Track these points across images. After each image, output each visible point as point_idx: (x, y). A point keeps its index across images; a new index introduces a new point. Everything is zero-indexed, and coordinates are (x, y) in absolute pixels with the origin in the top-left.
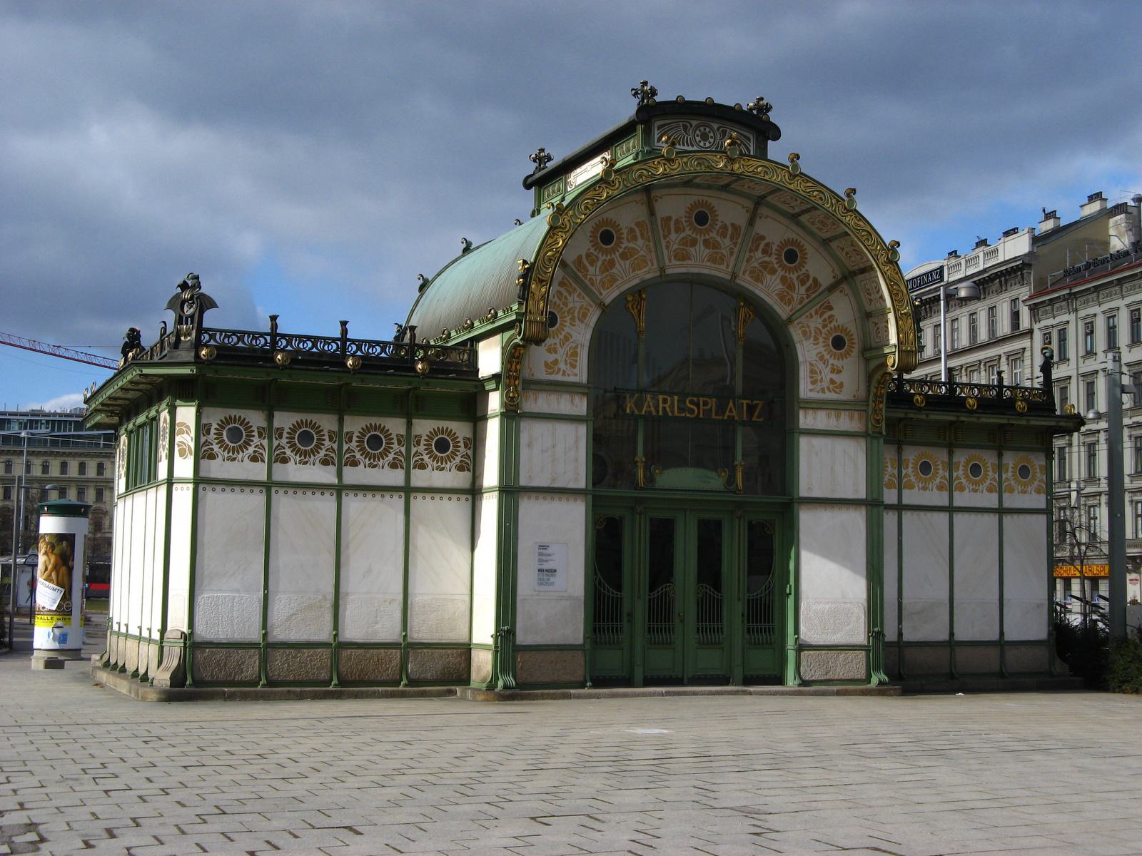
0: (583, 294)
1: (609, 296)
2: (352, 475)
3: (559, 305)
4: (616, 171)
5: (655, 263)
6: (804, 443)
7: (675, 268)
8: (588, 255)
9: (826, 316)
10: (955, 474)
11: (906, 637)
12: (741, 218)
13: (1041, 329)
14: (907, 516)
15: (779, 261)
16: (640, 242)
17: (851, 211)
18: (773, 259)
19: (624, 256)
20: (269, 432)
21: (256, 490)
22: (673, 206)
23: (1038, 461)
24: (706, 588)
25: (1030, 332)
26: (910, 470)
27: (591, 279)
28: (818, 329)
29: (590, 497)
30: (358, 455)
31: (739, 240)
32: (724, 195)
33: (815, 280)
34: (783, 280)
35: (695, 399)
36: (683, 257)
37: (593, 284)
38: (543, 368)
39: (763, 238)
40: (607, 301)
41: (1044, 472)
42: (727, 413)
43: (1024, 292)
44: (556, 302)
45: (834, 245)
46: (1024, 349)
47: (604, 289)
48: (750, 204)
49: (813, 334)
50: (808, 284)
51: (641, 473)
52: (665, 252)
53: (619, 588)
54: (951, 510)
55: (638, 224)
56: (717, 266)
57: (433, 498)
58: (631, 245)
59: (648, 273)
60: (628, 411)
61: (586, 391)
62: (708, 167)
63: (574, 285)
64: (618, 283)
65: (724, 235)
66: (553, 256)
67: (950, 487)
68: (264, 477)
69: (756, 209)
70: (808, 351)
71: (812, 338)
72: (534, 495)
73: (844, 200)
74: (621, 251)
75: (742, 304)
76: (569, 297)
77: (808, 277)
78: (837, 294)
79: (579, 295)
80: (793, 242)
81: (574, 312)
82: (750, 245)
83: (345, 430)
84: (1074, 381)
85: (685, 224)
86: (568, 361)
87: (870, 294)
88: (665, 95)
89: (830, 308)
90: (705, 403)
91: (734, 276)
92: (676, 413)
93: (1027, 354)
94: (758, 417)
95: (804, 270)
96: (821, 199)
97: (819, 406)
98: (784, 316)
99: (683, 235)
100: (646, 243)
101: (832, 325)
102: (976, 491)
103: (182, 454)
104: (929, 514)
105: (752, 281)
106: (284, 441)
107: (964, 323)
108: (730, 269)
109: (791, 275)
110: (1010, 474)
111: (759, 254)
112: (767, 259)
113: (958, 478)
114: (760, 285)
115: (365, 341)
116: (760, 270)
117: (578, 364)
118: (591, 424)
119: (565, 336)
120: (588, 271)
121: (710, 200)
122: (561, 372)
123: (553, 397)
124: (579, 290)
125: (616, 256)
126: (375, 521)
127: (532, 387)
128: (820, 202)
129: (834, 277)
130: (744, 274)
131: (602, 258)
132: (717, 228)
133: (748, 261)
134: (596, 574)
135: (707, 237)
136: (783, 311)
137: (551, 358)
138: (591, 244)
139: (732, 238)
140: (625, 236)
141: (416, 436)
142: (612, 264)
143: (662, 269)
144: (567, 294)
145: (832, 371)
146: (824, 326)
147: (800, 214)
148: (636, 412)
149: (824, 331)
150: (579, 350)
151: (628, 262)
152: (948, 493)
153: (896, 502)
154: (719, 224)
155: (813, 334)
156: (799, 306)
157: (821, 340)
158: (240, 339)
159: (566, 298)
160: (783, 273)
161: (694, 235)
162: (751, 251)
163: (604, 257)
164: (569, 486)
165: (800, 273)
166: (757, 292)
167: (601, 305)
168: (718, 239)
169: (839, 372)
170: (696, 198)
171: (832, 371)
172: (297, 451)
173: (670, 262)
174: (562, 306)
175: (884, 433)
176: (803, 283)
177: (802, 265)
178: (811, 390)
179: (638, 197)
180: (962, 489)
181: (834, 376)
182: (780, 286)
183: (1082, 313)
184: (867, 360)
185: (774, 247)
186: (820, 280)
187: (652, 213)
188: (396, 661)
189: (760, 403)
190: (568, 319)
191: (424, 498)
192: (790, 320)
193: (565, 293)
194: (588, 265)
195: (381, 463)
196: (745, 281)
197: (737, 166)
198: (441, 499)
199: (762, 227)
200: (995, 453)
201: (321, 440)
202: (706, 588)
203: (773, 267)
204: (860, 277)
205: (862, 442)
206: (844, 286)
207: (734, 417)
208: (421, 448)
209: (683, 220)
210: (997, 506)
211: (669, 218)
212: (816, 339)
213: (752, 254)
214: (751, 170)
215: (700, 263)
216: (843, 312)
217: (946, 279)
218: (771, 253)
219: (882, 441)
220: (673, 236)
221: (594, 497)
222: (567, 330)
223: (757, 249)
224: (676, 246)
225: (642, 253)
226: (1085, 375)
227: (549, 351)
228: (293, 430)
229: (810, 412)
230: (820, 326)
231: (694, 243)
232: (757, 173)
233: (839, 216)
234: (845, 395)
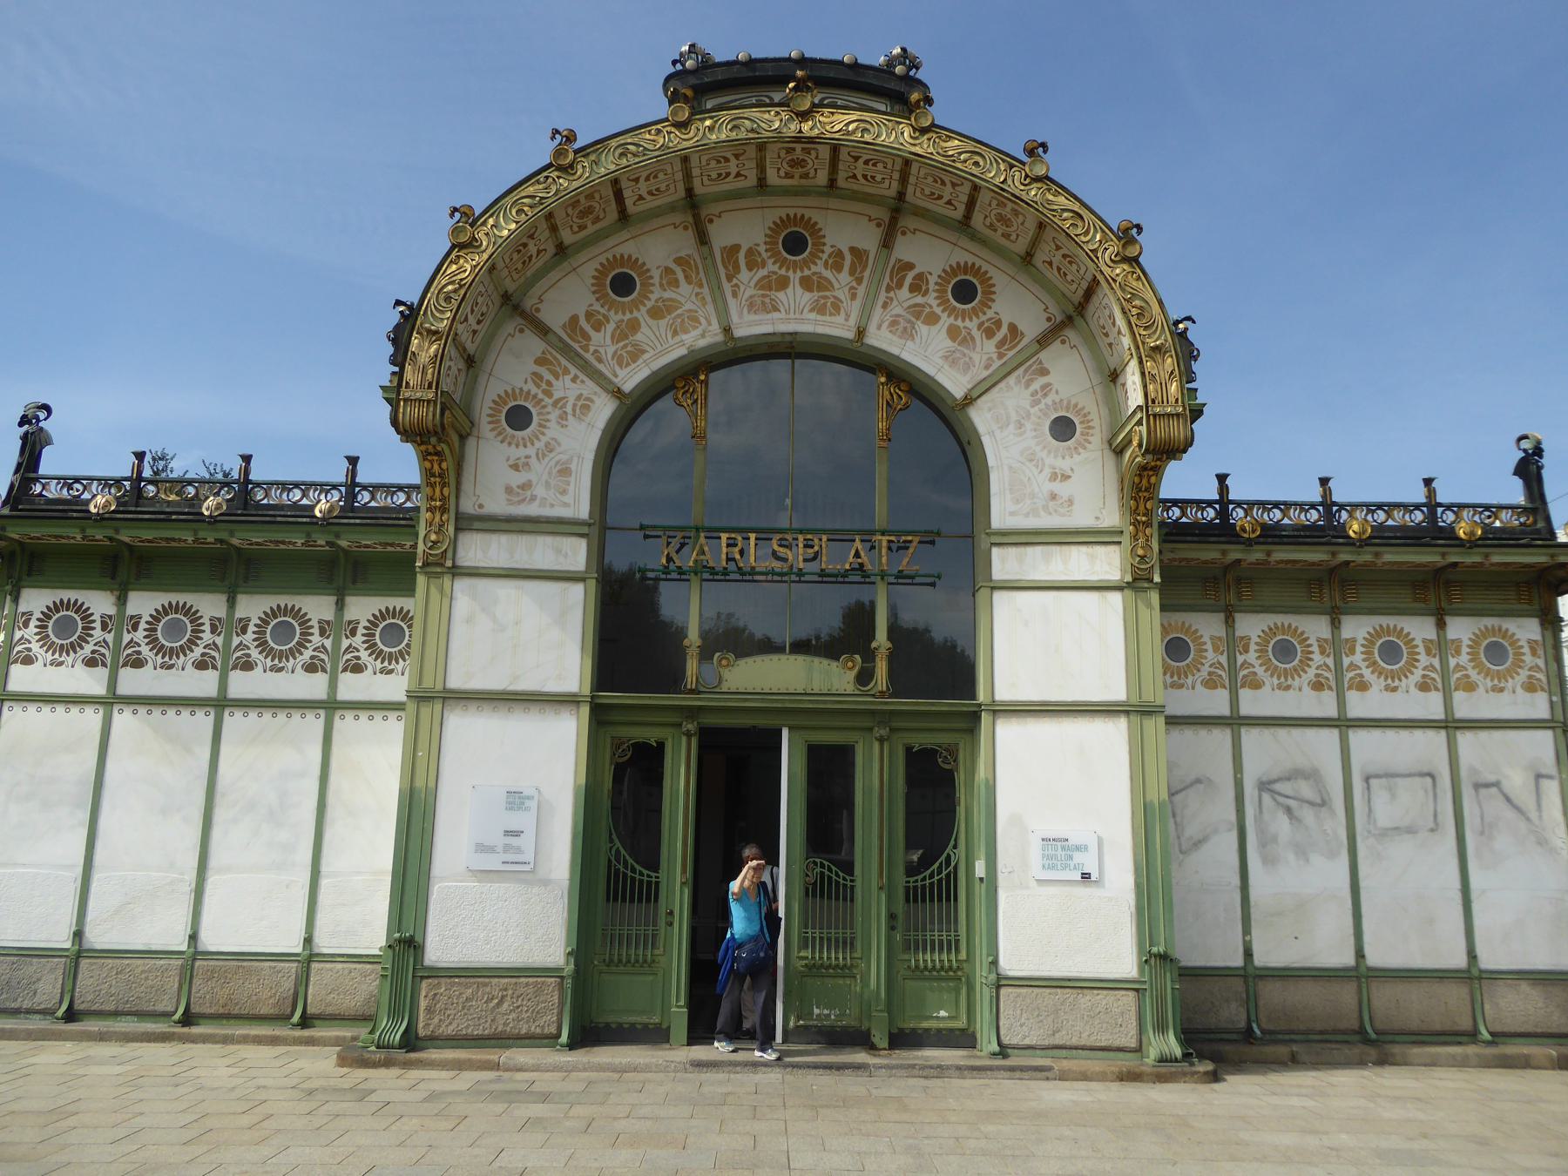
0: (582, 376)
1: (631, 378)
2: (242, 685)
3: (535, 396)
4: (576, 152)
5: (714, 321)
7: (751, 326)
8: (589, 315)
9: (1036, 385)
10: (1346, 661)
11: (1260, 960)
12: (869, 239)
14: (1249, 736)
15: (944, 302)
16: (685, 288)
17: (1037, 179)
18: (932, 299)
19: (656, 313)
20: (119, 622)
21: (89, 710)
22: (742, 229)
23: (1527, 630)
24: (822, 866)
26: (1252, 656)
27: (596, 351)
29: (585, 710)
30: (255, 654)
31: (867, 273)
32: (834, 203)
33: (1013, 328)
34: (953, 333)
35: (789, 537)
37: (600, 360)
38: (504, 496)
39: (910, 266)
40: (628, 387)
41: (1540, 652)
44: (529, 392)
45: (1039, 259)
47: (620, 364)
48: (885, 216)
49: (1014, 417)
50: (999, 336)
51: (692, 666)
52: (732, 302)
53: (655, 867)
54: (1343, 724)
55: (679, 261)
56: (828, 318)
57: (357, 718)
58: (666, 295)
59: (703, 336)
61: (585, 530)
62: (752, 130)
63: (564, 362)
64: (646, 356)
65: (838, 267)
66: (455, 291)
67: (1339, 682)
68: (100, 690)
69: (894, 221)
71: (1012, 427)
72: (473, 706)
73: (1023, 164)
74: (649, 304)
75: (883, 379)
76: (554, 382)
77: (998, 323)
78: (1057, 343)
79: (574, 380)
80: (966, 269)
81: (565, 405)
82: (887, 279)
83: (239, 614)
85: (765, 255)
86: (553, 482)
87: (1106, 335)
88: (721, 53)
89: (1044, 372)
91: (861, 333)
95: (990, 314)
96: (976, 164)
97: (1023, 539)
98: (959, 393)
99: (763, 272)
100: (697, 290)
101: (1049, 400)
102: (1395, 689)
104: (1297, 733)
105: (895, 338)
106: (140, 635)
108: (852, 321)
109: (968, 323)
110: (1464, 658)
111: (904, 293)
112: (919, 300)
113: (1353, 666)
114: (909, 343)
115: (277, 483)
116: (909, 321)
117: (571, 488)
118: (592, 584)
119: (547, 444)
120: (588, 338)
121: (808, 213)
122: (537, 502)
123: (523, 541)
124: (573, 371)
125: (641, 314)
127: (477, 525)
128: (975, 170)
129: (1049, 319)
130: (879, 327)
131: (615, 317)
132: (825, 256)
133: (885, 306)
134: (611, 841)
135: (807, 272)
136: (955, 383)
137: (516, 479)
138: (592, 299)
139: (852, 273)
140: (656, 280)
141: (350, 622)
142: (634, 326)
143: (727, 330)
144: (551, 378)
145: (1054, 477)
146: (1035, 403)
147: (968, 216)
149: (1032, 411)
150: (573, 467)
151: (663, 323)
152: (1334, 694)
153: (1226, 712)
154: (828, 250)
155: (1014, 417)
156: (986, 373)
157: (1029, 426)
158: (85, 488)
159: (549, 384)
161: (783, 272)
163: (620, 316)
164: (546, 689)
165: (983, 318)
166: (906, 356)
167: (617, 393)
168: (828, 274)
169: (1066, 477)
170: (783, 213)
171: (1054, 477)
172: (160, 650)
173: (741, 315)
174: (541, 396)
176: (989, 334)
177: (986, 304)
178: (1012, 514)
179: (678, 218)
180: (1363, 686)
181: (1057, 487)
182: (949, 343)
184: (1119, 452)
185: (933, 280)
186: (1020, 327)
187: (703, 239)
188: (288, 985)
190: (554, 415)
191: (357, 718)
192: (969, 400)
193: (548, 376)
194: (591, 332)
195: (290, 665)
196: (882, 339)
197: (806, 127)
198: (385, 718)
199: (904, 249)
201: (197, 631)
202: (822, 866)
203: (934, 313)
204: (1091, 308)
205: (1116, 598)
206: (1070, 333)
207: (862, 565)
208: (358, 640)
209: (762, 249)
210: (1442, 717)
211: (735, 248)
212: (1020, 425)
213: (892, 294)
214: (837, 128)
215: (795, 314)
216: (1067, 376)
218: (927, 291)
219: (1155, 597)
220: (744, 275)
222: (550, 433)
223: (900, 285)
224: (749, 292)
225: (688, 306)
227: (515, 467)
228: (156, 618)
229: (1012, 550)
230: (1026, 404)
231: (783, 284)
232: (848, 133)
233: (1017, 193)
234: (1082, 518)
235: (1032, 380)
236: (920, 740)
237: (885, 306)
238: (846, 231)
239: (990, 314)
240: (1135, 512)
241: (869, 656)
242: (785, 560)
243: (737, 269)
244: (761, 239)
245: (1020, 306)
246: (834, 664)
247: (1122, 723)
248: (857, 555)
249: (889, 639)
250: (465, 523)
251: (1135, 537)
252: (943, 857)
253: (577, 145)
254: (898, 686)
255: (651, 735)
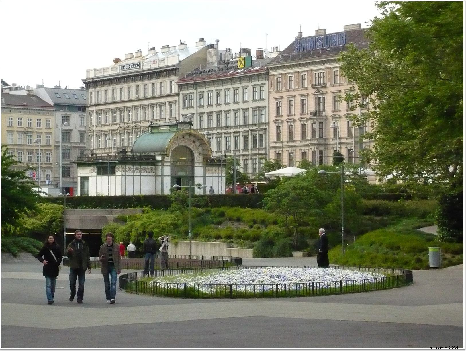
6: (195, 168)
12: (188, 137)
13: (183, 94)
25: (178, 95)
36: (181, 143)
43: (176, 79)
46: (176, 101)
67: (212, 173)
70: (196, 155)
84: (195, 116)
93: (177, 103)
107: (150, 87)
126: (144, 179)
136: (192, 149)
183: (199, 90)
196: (188, 146)
216: (200, 149)
217: (142, 67)
226: (200, 114)
238: (187, 137)
245: (197, 143)
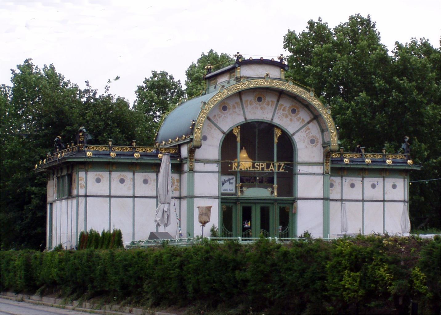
1: (226, 129)
9: (307, 132)
28: (305, 137)
29: (220, 199)
35: (258, 164)
42: (270, 168)
55: (236, 103)
60: (233, 169)
77: (300, 118)
89: (309, 129)
90: (262, 165)
92: (251, 169)
94: (282, 169)
101: (310, 135)
103: (81, 187)
124: (215, 127)
133: (277, 113)
146: (307, 136)
148: (236, 169)
154: (266, 101)
160: (291, 117)
162: (278, 110)
167: (224, 133)
175: (330, 173)
184: (324, 147)
189: (283, 164)
192: (294, 134)
193: (210, 129)
194: (219, 119)
196: (276, 121)
200: (382, 179)
205: (322, 176)
209: (253, 101)
221: (222, 199)
235: (307, 131)
236: (282, 206)
237: (277, 113)
239: (298, 116)
240: (326, 160)
241: (273, 188)
242: (257, 168)
243: (248, 104)
244: (253, 99)
246: (266, 190)
247: (322, 201)
248: (272, 167)
249: (277, 184)
250: (197, 161)
251: (326, 165)
252: (286, 229)
253: (225, 88)
254: (279, 194)
255: (230, 205)
